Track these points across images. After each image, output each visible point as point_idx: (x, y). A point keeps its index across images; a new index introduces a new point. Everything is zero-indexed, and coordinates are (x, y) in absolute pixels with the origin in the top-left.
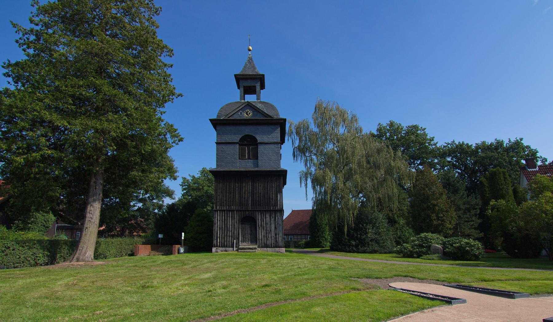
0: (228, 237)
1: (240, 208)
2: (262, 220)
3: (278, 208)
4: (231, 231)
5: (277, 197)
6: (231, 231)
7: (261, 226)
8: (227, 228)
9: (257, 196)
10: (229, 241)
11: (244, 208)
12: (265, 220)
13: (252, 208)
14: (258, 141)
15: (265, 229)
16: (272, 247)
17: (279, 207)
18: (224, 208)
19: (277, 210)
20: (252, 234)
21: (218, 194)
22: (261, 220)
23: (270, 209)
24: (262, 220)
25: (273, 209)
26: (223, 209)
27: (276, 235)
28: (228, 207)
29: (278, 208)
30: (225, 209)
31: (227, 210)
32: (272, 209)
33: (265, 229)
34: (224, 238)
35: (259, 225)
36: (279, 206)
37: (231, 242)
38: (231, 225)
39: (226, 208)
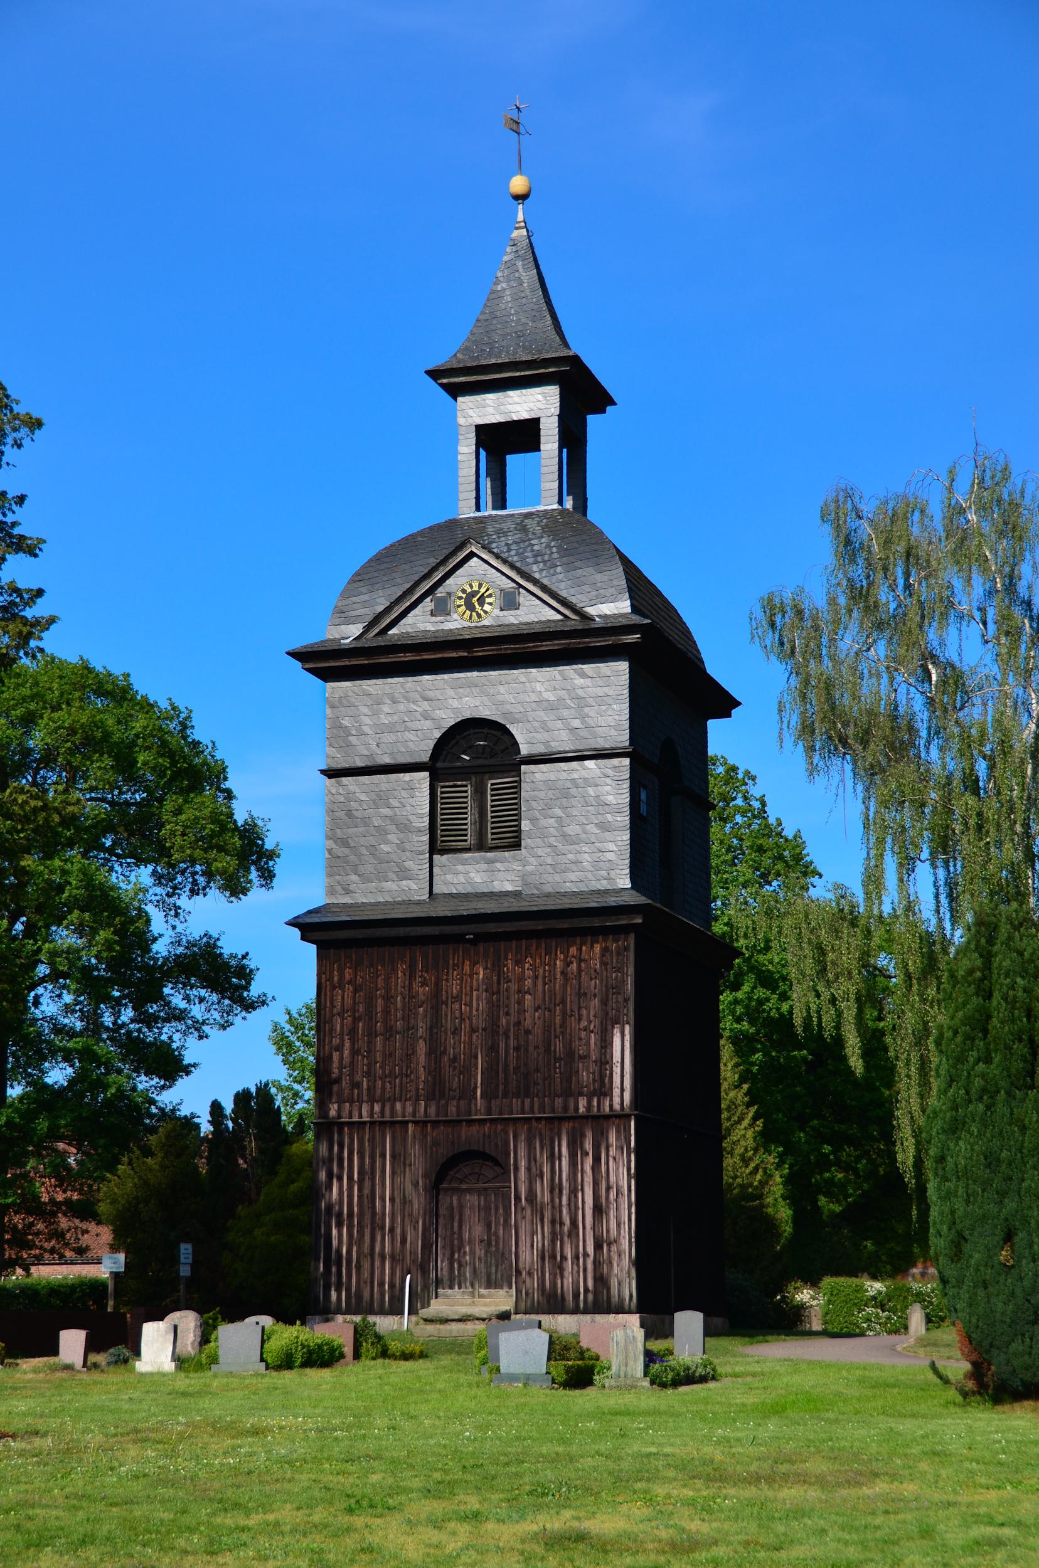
0: (377, 1263)
1: (432, 1110)
2: (534, 1175)
3: (611, 1106)
4: (392, 1230)
5: (606, 1044)
6: (392, 1230)
7: (531, 1197)
8: (374, 1213)
9: (512, 1043)
10: (382, 1284)
11: (452, 1109)
12: (546, 1169)
13: (489, 1112)
14: (524, 750)
15: (547, 1215)
16: (576, 1311)
17: (617, 1100)
18: (360, 1116)
19: (607, 1117)
20: (489, 1244)
21: (336, 1041)
22: (529, 1169)
23: (577, 1109)
24: (534, 1175)
25: (589, 1107)
26: (356, 1119)
27: (598, 1246)
28: (377, 1108)
29: (611, 1106)
30: (366, 1119)
31: (372, 1123)
32: (582, 1110)
33: (547, 1215)
34: (359, 1267)
35: (518, 1198)
36: (616, 1092)
37: (392, 1286)
38: (392, 1200)
39: (372, 1115)
